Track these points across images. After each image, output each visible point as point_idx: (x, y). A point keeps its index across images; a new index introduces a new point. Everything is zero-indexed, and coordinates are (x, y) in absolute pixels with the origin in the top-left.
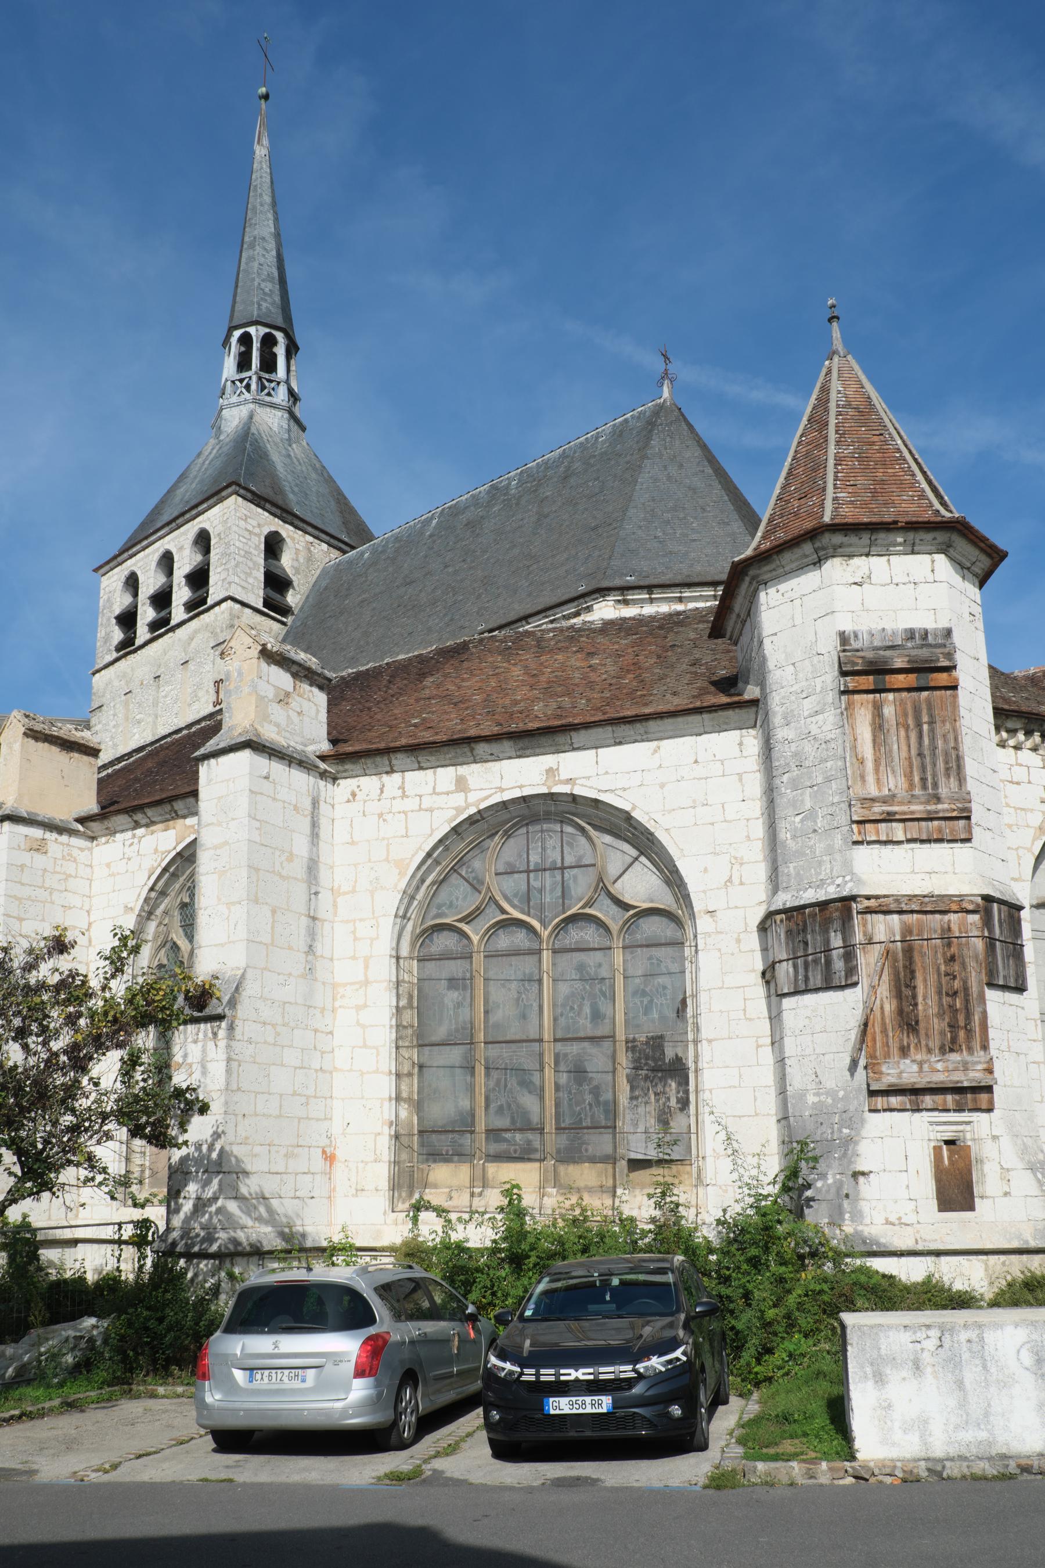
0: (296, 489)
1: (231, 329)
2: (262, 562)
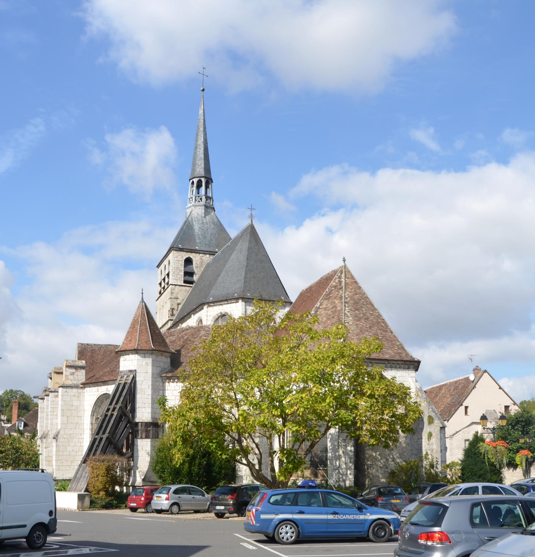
0: (201, 237)
1: (190, 180)
2: (183, 269)
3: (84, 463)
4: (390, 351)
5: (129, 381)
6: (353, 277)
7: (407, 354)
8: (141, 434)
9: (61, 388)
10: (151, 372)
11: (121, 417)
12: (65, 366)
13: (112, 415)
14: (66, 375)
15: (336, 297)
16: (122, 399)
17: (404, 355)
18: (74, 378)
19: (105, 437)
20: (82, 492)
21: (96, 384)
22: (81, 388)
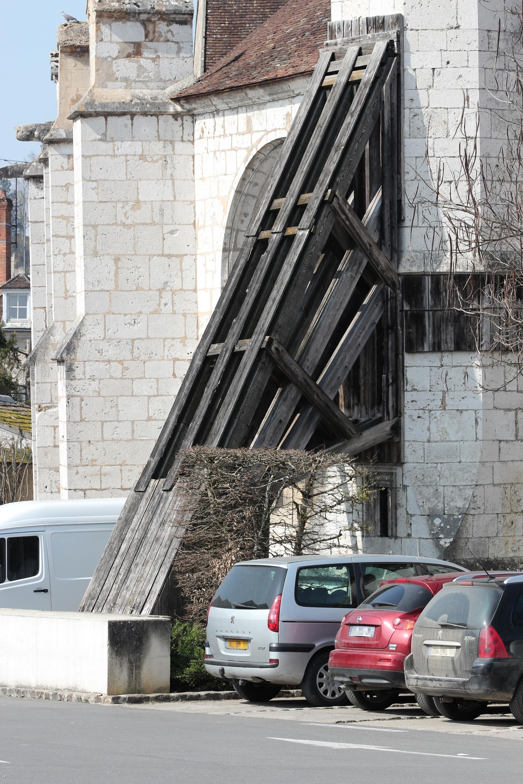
3: (155, 476)
5: (367, 76)
8: (437, 331)
9: (78, 125)
10: (475, 24)
11: (333, 249)
12: (93, 15)
13: (287, 241)
14: (100, 60)
16: (330, 165)
18: (140, 67)
19: (250, 347)
20: (146, 615)
21: (239, 96)
22: (176, 116)
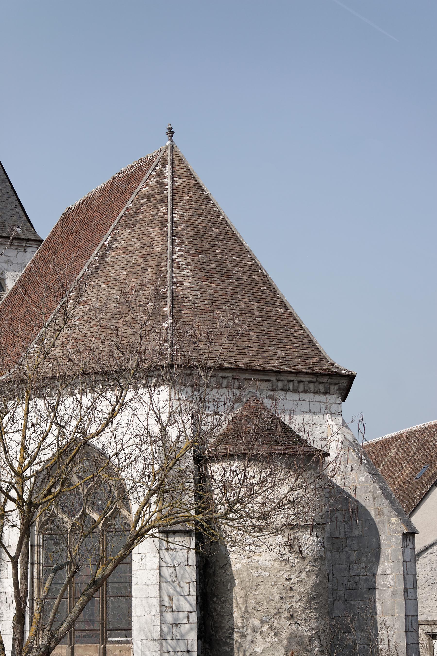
4: (282, 352)
6: (190, 175)
7: (322, 359)
15: (150, 222)
17: (314, 360)
